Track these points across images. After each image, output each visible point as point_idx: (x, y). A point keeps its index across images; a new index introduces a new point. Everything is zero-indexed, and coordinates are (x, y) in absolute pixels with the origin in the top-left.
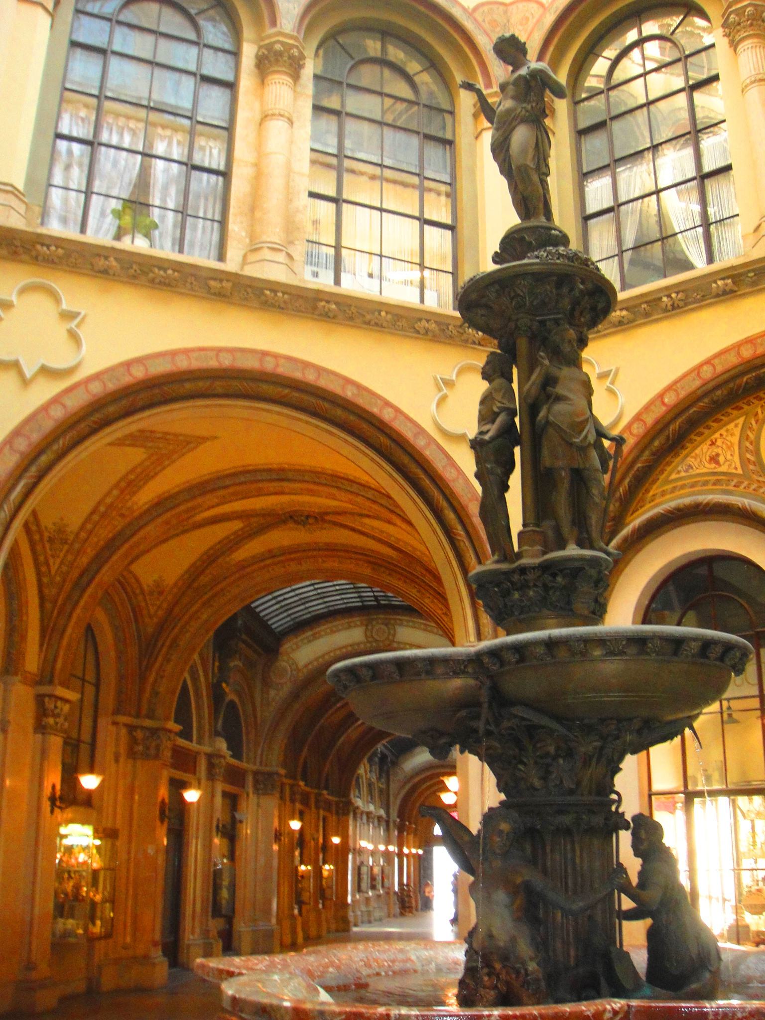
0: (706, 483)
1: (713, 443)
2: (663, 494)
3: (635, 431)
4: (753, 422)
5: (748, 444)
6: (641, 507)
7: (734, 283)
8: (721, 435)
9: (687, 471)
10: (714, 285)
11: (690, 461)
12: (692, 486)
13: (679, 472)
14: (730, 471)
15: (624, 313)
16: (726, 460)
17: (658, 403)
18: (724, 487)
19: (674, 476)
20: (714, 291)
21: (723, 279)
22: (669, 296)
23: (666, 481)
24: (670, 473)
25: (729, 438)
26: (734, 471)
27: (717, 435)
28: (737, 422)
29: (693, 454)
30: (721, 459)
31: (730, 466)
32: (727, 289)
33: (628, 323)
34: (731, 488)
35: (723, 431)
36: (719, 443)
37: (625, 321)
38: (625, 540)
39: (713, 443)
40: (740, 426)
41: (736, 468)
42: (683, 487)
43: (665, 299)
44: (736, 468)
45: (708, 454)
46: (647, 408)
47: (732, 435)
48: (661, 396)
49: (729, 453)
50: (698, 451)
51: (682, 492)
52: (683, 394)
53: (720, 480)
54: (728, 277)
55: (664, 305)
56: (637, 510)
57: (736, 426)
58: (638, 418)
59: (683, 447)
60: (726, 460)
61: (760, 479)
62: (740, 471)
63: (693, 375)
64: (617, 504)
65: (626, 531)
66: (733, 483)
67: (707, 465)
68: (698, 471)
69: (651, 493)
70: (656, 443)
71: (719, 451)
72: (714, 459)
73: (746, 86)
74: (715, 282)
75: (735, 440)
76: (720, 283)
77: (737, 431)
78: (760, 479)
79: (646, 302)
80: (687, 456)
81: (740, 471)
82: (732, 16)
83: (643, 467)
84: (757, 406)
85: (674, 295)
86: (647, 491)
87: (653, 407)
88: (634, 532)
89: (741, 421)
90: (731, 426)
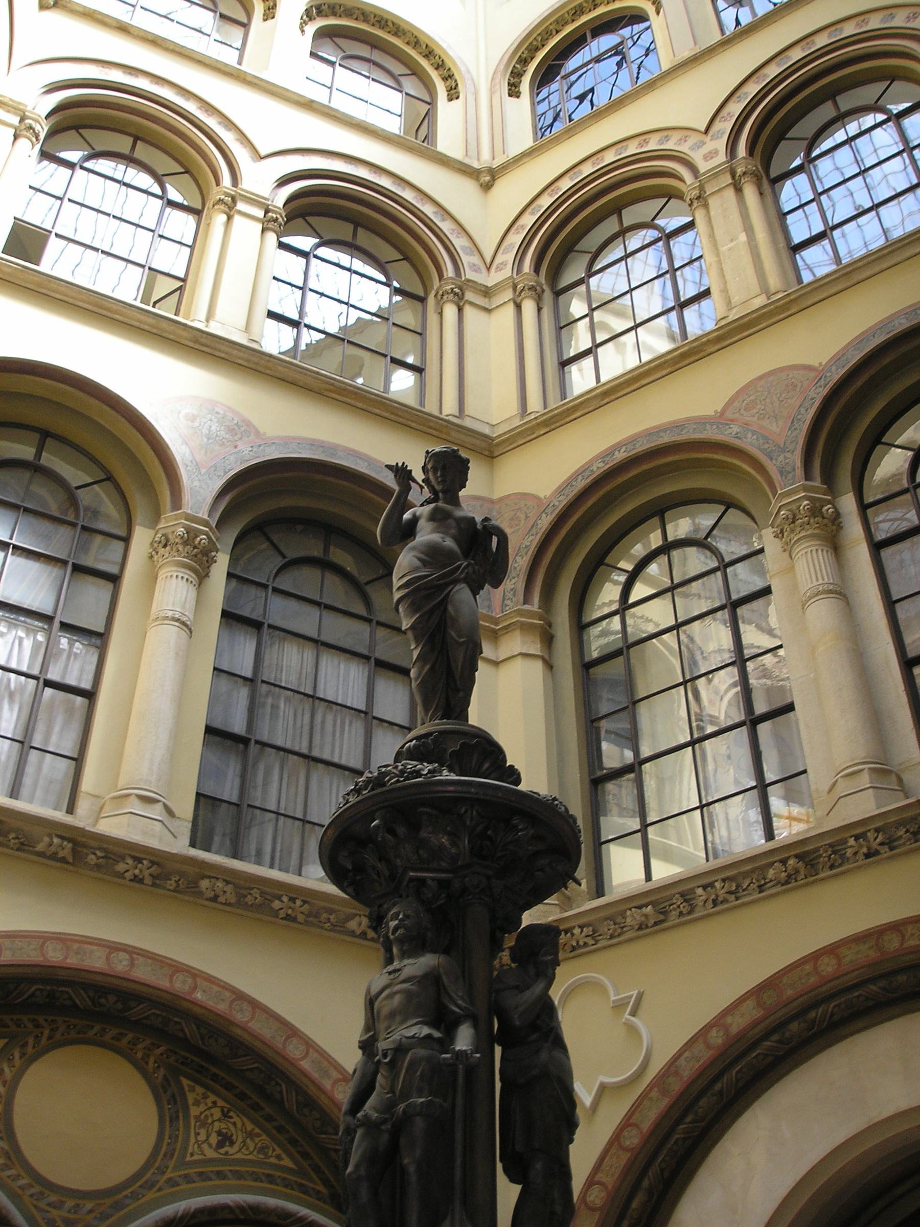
4: (17, 1054)
7: (74, 851)
10: (46, 839)
20: (40, 847)
21: (62, 838)
54: (69, 840)
74: (50, 836)
76: (56, 841)
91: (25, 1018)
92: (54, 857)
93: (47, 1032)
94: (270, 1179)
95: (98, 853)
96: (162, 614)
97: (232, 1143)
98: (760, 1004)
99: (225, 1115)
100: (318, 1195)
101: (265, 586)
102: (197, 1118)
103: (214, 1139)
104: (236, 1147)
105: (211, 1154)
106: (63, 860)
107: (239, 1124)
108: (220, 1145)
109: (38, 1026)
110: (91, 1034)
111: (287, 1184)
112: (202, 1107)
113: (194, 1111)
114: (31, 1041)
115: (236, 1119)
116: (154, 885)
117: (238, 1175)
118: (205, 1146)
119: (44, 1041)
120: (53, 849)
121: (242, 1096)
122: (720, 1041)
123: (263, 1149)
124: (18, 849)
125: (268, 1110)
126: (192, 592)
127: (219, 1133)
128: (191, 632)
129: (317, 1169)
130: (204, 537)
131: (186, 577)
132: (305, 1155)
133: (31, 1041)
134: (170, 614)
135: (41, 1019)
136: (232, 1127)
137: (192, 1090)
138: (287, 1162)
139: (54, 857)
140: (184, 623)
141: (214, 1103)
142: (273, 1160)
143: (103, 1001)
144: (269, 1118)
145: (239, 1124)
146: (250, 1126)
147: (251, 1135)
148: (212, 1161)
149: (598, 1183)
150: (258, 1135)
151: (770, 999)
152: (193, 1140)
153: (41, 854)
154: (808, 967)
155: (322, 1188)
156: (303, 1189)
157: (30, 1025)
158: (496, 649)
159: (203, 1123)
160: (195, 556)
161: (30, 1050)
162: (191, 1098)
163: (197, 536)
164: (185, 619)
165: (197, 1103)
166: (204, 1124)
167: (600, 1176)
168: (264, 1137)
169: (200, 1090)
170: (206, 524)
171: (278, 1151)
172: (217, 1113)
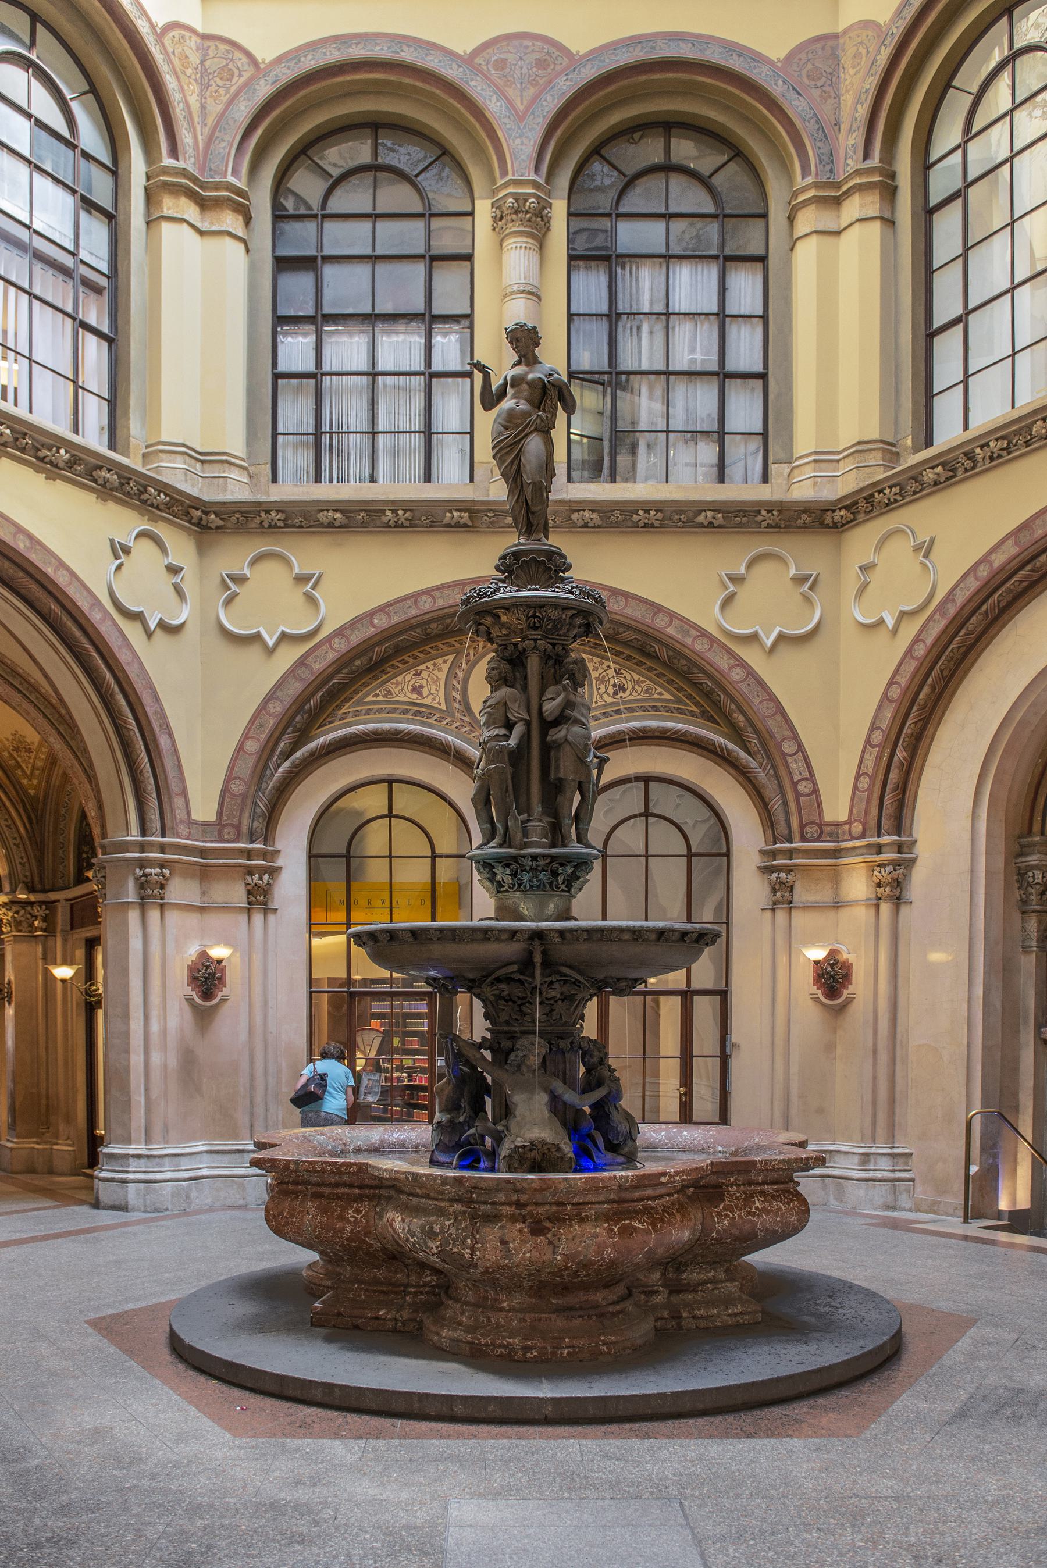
0: (405, 712)
2: (357, 713)
4: (464, 662)
6: (330, 722)
8: (427, 668)
9: (385, 696)
11: (390, 686)
13: (377, 695)
16: (430, 693)
18: (425, 719)
19: (369, 698)
24: (367, 695)
25: (436, 672)
26: (437, 706)
27: (423, 667)
28: (446, 658)
29: (394, 681)
30: (425, 692)
31: (434, 699)
34: (432, 721)
35: (429, 664)
36: (424, 674)
38: (312, 753)
39: (417, 674)
40: (449, 663)
41: (440, 704)
44: (440, 704)
45: (412, 683)
49: (434, 687)
50: (400, 678)
56: (325, 725)
57: (445, 662)
59: (383, 672)
60: (430, 693)
61: (464, 718)
62: (443, 707)
64: (306, 716)
65: (313, 745)
66: (435, 718)
67: (409, 694)
69: (342, 711)
70: (358, 663)
71: (424, 683)
72: (417, 690)
75: (442, 676)
77: (446, 667)
78: (464, 718)
81: (443, 707)
83: (339, 684)
86: (339, 707)
88: (323, 747)
89: (451, 658)
90: (440, 661)
94: (655, 708)
96: (509, 290)
97: (624, 690)
99: (618, 673)
100: (692, 714)
101: (609, 215)
102: (597, 679)
103: (611, 690)
104: (628, 693)
105: (609, 700)
107: (628, 677)
108: (615, 693)
111: (668, 710)
112: (600, 671)
113: (594, 674)
115: (626, 674)
117: (631, 710)
118: (605, 696)
119: (480, 649)
121: (629, 658)
123: (647, 691)
125: (649, 664)
126: (535, 257)
127: (614, 685)
128: (539, 297)
129: (690, 697)
130: (533, 200)
131: (524, 245)
132: (680, 689)
134: (515, 288)
136: (623, 680)
137: (591, 661)
138: (666, 696)
140: (530, 293)
141: (609, 667)
142: (656, 696)
144: (650, 669)
145: (628, 677)
146: (636, 677)
147: (638, 683)
148: (611, 704)
150: (644, 682)
152: (595, 693)
155: (695, 709)
156: (680, 711)
159: (602, 680)
160: (529, 220)
162: (590, 666)
163: (526, 200)
164: (529, 288)
165: (596, 669)
166: (603, 682)
168: (648, 682)
169: (597, 660)
170: (535, 184)
171: (660, 690)
172: (611, 673)
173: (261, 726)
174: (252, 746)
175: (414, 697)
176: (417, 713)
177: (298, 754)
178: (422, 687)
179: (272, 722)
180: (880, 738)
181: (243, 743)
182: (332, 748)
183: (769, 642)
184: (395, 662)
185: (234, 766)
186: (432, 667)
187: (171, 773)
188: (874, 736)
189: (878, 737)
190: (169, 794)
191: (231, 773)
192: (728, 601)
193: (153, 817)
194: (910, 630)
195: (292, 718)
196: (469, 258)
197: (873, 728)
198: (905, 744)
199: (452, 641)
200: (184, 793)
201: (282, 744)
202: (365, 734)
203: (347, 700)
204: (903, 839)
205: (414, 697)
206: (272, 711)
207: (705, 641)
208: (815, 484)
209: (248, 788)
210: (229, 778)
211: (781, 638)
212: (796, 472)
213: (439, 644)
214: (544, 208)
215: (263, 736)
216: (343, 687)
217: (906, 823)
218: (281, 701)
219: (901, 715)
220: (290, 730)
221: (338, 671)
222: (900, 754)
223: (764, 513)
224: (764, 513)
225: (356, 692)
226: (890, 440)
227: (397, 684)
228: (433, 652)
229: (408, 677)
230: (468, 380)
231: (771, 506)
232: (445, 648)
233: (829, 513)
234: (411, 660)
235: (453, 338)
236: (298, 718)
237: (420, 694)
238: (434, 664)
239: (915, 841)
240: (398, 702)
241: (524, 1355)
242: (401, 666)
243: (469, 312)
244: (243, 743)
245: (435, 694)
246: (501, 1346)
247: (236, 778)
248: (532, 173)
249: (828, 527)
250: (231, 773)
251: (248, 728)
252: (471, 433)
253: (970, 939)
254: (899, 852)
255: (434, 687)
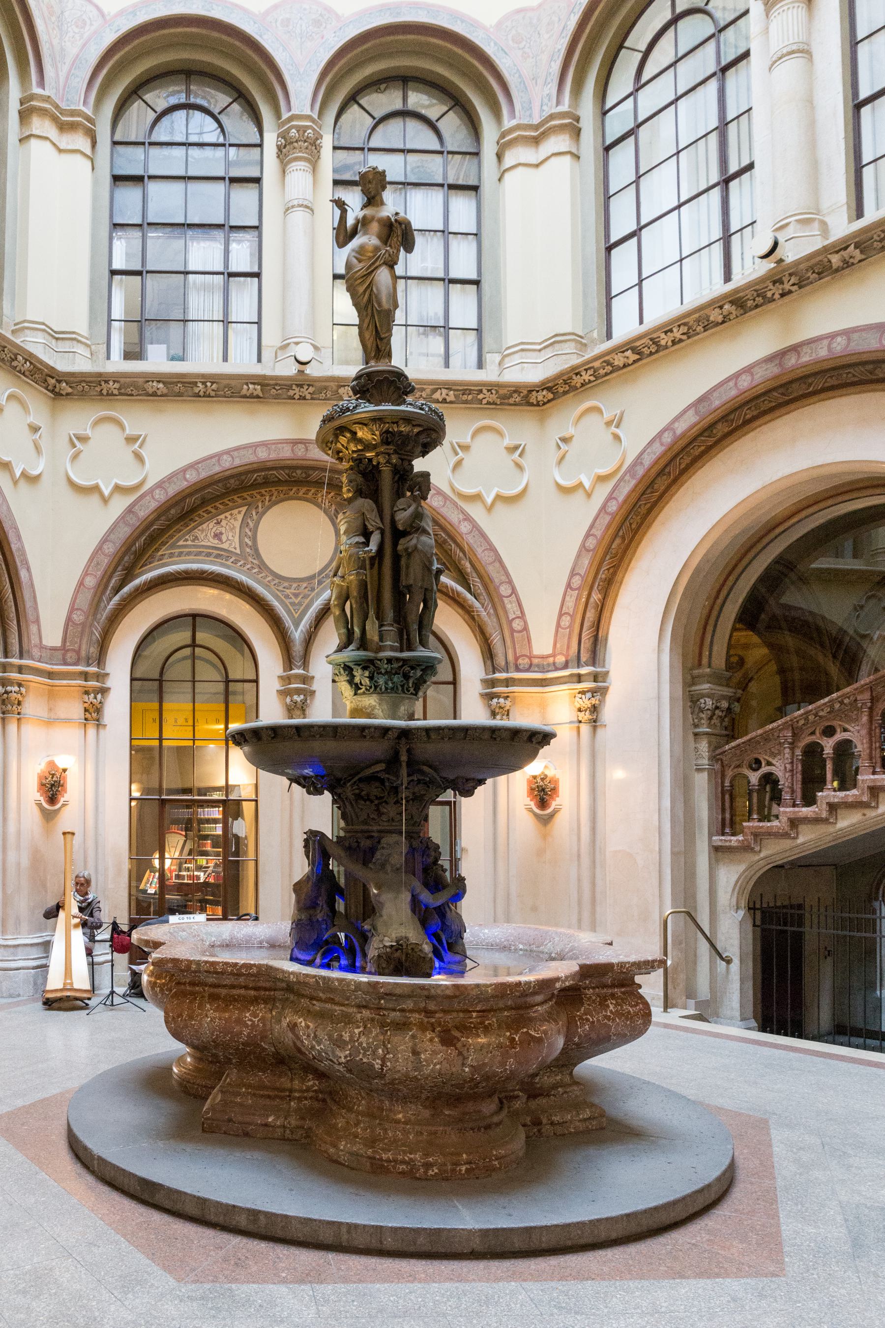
0: (209, 555)
1: (218, 523)
2: (171, 555)
3: (157, 497)
4: (254, 513)
5: (247, 530)
6: (150, 563)
8: (226, 517)
9: (193, 541)
10: (245, 387)
11: (197, 532)
12: (198, 554)
13: (187, 540)
14: (230, 549)
15: (161, 385)
16: (228, 539)
17: (180, 476)
22: (204, 383)
23: (173, 546)
24: (178, 541)
26: (233, 550)
27: (222, 516)
28: (240, 509)
29: (200, 528)
30: (224, 538)
31: (230, 545)
32: (255, 393)
33: (161, 396)
34: (229, 563)
35: (227, 514)
36: (224, 523)
37: (159, 393)
39: (218, 523)
40: (243, 513)
41: (235, 548)
42: (189, 554)
43: (200, 385)
44: (235, 548)
46: (170, 478)
47: (235, 519)
48: (184, 470)
49: (231, 534)
50: (204, 526)
51: (187, 557)
52: (204, 475)
53: (221, 555)
54: (258, 384)
55: (196, 390)
56: (146, 565)
57: (239, 512)
58: (160, 485)
60: (228, 539)
61: (254, 561)
62: (238, 551)
63: (214, 460)
64: (132, 557)
65: (137, 582)
66: (232, 560)
67: (211, 539)
68: (203, 543)
69: (160, 553)
70: (173, 511)
72: (218, 536)
73: (293, 207)
74: (247, 384)
75: (237, 524)
76: (251, 386)
77: (240, 517)
79: (182, 383)
80: (194, 528)
81: (238, 551)
82: (293, 130)
83: (158, 529)
84: (258, 500)
85: (209, 384)
86: (157, 550)
87: (175, 479)
89: (244, 509)
90: (235, 511)
91: (254, 492)
92: (251, 396)
93: (267, 498)
95: (277, 388)
98: (696, 413)
106: (258, 397)
109: (262, 495)
110: (291, 493)
114: (260, 505)
116: (312, 399)
119: (267, 503)
120: (250, 392)
122: (669, 440)
124: (231, 397)
133: (260, 505)
135: (263, 491)
139: (251, 396)
143: (294, 474)
149: (592, 535)
151: (704, 409)
153: (245, 397)
154: (731, 384)
157: (259, 497)
158: (537, 152)
161: (260, 509)
164: (305, 203)
167: (594, 531)
170: (308, 118)
173: (98, 564)
174: (91, 582)
175: (215, 542)
176: (218, 556)
177: (126, 589)
178: (221, 533)
179: (106, 561)
180: (579, 582)
181: (83, 578)
182: (152, 584)
183: (489, 500)
184: (201, 512)
185: (76, 598)
186: (229, 517)
187: (29, 604)
188: (573, 581)
189: (577, 581)
190: (27, 621)
191: (74, 604)
192: (458, 465)
193: (14, 641)
194: (602, 493)
195: (121, 559)
196: (257, 181)
197: (573, 574)
198: (600, 588)
199: (245, 495)
200: (37, 621)
201: (113, 581)
202: (178, 573)
203: (163, 544)
204: (599, 670)
205: (215, 542)
206: (107, 551)
207: (440, 498)
208: (523, 369)
209: (87, 618)
210: (72, 609)
211: (498, 497)
212: (507, 359)
213: (235, 497)
214: (317, 139)
215: (99, 573)
216: (162, 532)
217: (600, 655)
218: (114, 543)
219: (596, 563)
220: (120, 568)
221: (157, 518)
222: (596, 596)
223: (485, 391)
224: (485, 391)
225: (171, 537)
226: (580, 334)
227: (203, 531)
228: (231, 504)
229: (211, 525)
230: (256, 279)
231: (491, 387)
232: (240, 501)
233: (534, 393)
234: (213, 510)
235: (246, 245)
236: (126, 558)
237: (220, 540)
238: (231, 515)
239: (608, 672)
240: (203, 546)
241: (426, 1172)
242: (205, 514)
243: (256, 224)
244: (83, 578)
245: (231, 540)
246: (403, 1162)
247: (77, 609)
248: (309, 109)
249: (532, 405)
250: (74, 604)
251: (88, 566)
252: (259, 323)
253: (659, 757)
254: (595, 681)
255: (231, 534)
